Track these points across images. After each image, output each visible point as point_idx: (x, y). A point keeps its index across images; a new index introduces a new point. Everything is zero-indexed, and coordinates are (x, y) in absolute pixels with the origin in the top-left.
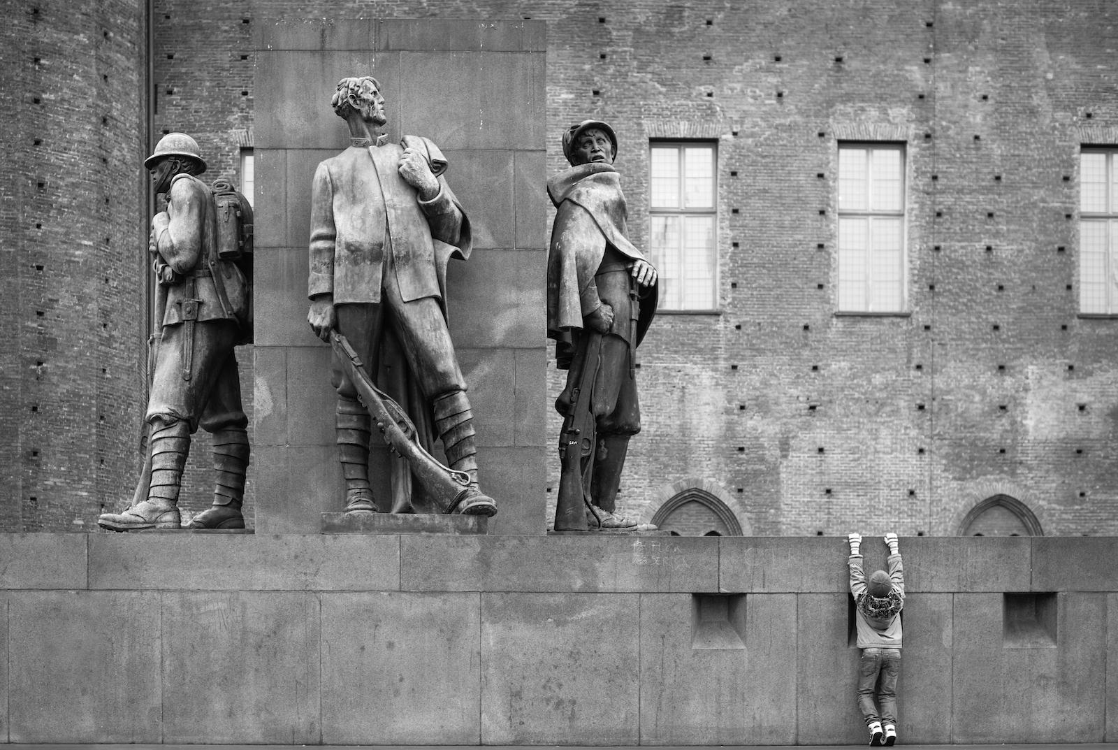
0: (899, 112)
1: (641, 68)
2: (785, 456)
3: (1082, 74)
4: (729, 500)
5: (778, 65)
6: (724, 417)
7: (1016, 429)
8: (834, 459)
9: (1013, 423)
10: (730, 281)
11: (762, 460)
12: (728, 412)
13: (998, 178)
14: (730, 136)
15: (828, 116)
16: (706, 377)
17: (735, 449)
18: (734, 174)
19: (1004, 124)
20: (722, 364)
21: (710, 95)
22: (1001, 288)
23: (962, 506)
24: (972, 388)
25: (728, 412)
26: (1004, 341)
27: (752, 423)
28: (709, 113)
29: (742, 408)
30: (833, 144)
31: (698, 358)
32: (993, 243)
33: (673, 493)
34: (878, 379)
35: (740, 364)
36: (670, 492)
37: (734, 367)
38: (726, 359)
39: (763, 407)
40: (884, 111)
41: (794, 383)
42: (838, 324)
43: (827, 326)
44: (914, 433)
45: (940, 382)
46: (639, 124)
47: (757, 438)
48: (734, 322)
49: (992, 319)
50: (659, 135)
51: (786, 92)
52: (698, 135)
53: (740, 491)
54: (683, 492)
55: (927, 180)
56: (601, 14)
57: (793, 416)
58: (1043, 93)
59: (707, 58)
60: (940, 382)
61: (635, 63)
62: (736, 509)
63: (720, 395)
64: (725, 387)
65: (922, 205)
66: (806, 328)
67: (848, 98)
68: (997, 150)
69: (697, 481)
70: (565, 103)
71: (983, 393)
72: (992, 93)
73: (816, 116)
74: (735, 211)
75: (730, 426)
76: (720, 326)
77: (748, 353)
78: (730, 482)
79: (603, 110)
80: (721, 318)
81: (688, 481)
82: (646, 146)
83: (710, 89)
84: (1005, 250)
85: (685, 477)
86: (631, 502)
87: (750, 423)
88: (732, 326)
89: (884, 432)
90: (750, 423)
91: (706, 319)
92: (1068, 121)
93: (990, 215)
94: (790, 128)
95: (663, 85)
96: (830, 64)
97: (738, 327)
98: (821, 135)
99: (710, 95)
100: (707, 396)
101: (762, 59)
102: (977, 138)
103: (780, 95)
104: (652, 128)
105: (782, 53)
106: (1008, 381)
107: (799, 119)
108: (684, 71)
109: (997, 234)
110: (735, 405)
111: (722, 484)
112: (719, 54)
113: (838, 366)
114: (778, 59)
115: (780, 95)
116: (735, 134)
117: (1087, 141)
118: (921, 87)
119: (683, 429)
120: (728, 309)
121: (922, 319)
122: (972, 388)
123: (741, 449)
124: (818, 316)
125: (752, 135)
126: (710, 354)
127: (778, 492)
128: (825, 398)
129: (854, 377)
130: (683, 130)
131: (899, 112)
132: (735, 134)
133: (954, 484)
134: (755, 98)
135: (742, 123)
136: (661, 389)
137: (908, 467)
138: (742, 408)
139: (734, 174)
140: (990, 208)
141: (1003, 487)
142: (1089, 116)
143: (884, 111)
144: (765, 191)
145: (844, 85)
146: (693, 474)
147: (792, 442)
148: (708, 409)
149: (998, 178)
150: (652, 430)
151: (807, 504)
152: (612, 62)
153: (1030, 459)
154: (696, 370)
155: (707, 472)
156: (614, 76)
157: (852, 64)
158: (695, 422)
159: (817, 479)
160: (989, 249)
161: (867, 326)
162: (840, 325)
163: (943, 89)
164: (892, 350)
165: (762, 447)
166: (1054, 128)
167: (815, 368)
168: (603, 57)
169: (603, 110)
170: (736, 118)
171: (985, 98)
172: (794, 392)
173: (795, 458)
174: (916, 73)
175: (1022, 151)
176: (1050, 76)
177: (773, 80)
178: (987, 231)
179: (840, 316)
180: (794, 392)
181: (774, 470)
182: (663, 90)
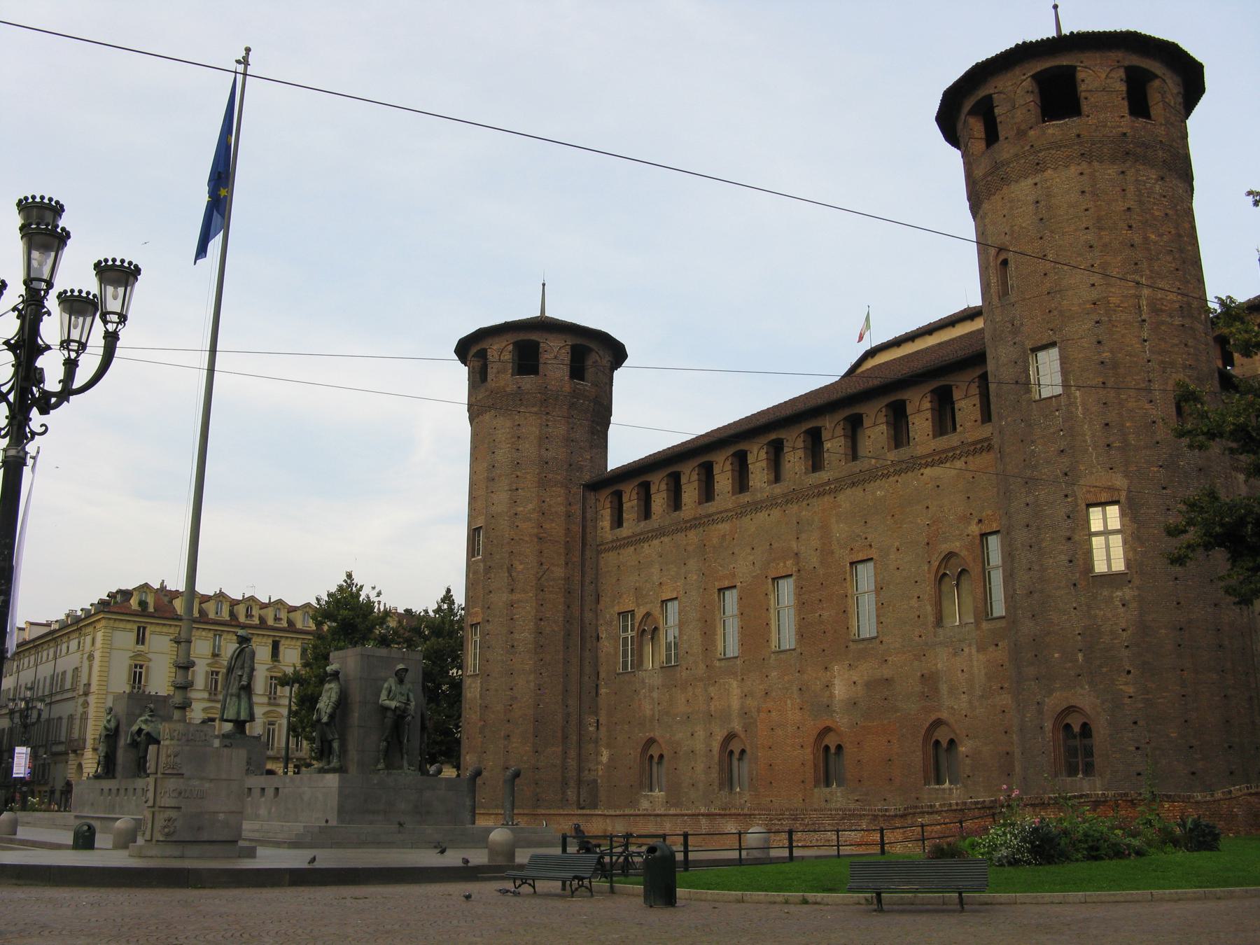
0: (789, 563)
7: (832, 696)
17: (745, 713)
23: (815, 733)
27: (749, 701)
28: (734, 575)
45: (805, 677)
84: (826, 614)
104: (718, 585)
113: (774, 674)
119: (729, 706)
141: (828, 723)
157: (774, 546)
173: (763, 715)
174: (794, 545)
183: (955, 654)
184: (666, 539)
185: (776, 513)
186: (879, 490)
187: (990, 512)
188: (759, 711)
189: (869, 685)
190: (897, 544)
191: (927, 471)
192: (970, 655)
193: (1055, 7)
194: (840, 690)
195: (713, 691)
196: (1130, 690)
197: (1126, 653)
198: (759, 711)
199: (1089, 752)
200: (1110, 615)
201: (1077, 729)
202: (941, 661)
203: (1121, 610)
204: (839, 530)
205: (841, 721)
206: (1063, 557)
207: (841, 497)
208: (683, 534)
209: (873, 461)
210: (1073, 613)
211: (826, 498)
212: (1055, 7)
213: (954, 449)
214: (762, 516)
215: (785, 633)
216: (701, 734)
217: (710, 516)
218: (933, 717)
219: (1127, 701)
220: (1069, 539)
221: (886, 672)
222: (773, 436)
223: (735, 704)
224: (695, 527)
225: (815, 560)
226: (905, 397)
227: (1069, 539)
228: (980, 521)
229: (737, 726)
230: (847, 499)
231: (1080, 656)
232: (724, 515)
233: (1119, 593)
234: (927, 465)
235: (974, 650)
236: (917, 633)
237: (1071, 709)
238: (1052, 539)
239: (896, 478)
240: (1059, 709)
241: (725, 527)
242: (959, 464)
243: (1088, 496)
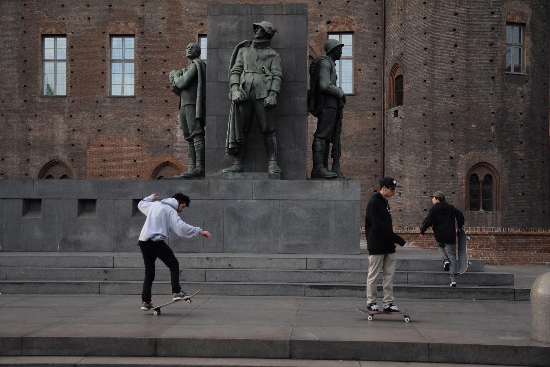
0: (132, 25)
1: (39, 9)
2: (89, 148)
3: (199, 9)
4: (68, 164)
5: (88, 8)
6: (67, 134)
8: (107, 148)
9: (172, 135)
10: (70, 85)
11: (80, 149)
12: (68, 132)
13: (168, 47)
14: (70, 34)
15: (106, 26)
16: (61, 119)
17: (71, 145)
18: (72, 47)
19: (170, 28)
20: (67, 115)
21: (64, 19)
22: (168, 87)
23: (154, 166)
24: (157, 123)
25: (68, 132)
26: (169, 106)
27: (77, 135)
28: (63, 25)
29: (74, 130)
30: (108, 36)
31: (58, 112)
32: (165, 70)
33: (48, 161)
34: (123, 120)
35: (73, 115)
36: (47, 160)
37: (71, 116)
38: (68, 113)
40: (126, 24)
41: (93, 122)
42: (109, 100)
43: (105, 101)
44: (136, 139)
45: (145, 121)
46: (38, 29)
47: (79, 141)
48: (71, 100)
49: (165, 98)
50: (45, 33)
51: (91, 17)
52: (59, 33)
53: (73, 160)
54: (52, 161)
55: (142, 48)
57: (92, 133)
58: (185, 16)
59: (63, 6)
60: (145, 121)
61: (37, 7)
62: (71, 167)
63: (66, 125)
64: (68, 123)
65: (140, 57)
66: (97, 102)
67: (113, 19)
68: (168, 37)
69: (57, 156)
70: (11, 22)
71: (161, 124)
72: (166, 17)
73: (102, 26)
74: (72, 60)
75: (69, 137)
76: (66, 101)
77: (76, 111)
78: (69, 157)
79: (25, 25)
80: (67, 98)
81: (54, 156)
82: (40, 37)
83: (64, 16)
85: (52, 155)
86: (33, 164)
87: (76, 136)
88: (70, 101)
89: (125, 139)
90: (76, 136)
91: (61, 99)
92: (194, 26)
93: (165, 61)
94: (92, 30)
95: (47, 15)
96: (107, 7)
97: (73, 102)
98: (104, 33)
99: (64, 19)
100: (61, 126)
101: (83, 6)
102: (160, 33)
103: (89, 19)
104: (42, 31)
105: (90, 3)
106: (171, 120)
107: (95, 27)
108: (54, 10)
109: (167, 68)
110: (71, 129)
111: (66, 158)
113: (109, 115)
114: (88, 6)
115: (89, 19)
116: (72, 33)
117: (201, 33)
119: (53, 138)
120: (69, 95)
121: (139, 98)
122: (157, 123)
123: (73, 145)
124: (102, 97)
125: (79, 33)
126: (62, 112)
127: (86, 161)
128: (104, 127)
129: (114, 119)
130: (54, 31)
132: (72, 33)
133: (150, 158)
134: (80, 20)
135: (75, 29)
136: (44, 124)
137: (134, 151)
138: (74, 130)
139: (72, 47)
140: (165, 58)
141: (168, 159)
142: (202, 24)
143: (126, 24)
144: (83, 53)
145: (112, 15)
146: (56, 154)
147: (91, 143)
148: (61, 131)
149: (168, 47)
150: (41, 138)
151: (96, 165)
152: (28, 7)
153: (178, 148)
154: (57, 117)
155: (60, 153)
156: (29, 12)
157: (115, 7)
158: (56, 135)
159: (100, 156)
160: (164, 73)
162: (109, 101)
163: (148, 15)
164: (128, 110)
165: (80, 144)
166: (189, 29)
167: (100, 116)
168: (25, 5)
169: (25, 25)
170: (73, 27)
171: (163, 18)
172: (93, 125)
173: (94, 148)
174: (138, 11)
175: (177, 37)
176: (187, 10)
177: (86, 13)
178: (164, 67)
180: (93, 125)
181: (85, 153)
182: (47, 17)
187: (338, 17)
188: (89, 144)
195: (31, 123)
196: (522, 154)
197: (521, 130)
198: (89, 144)
199: (487, 195)
200: (514, 102)
201: (481, 178)
203: (521, 100)
206: (485, 57)
210: (490, 97)
215: (123, 82)
219: (520, 162)
220: (492, 44)
223: (61, 135)
225: (161, 27)
227: (492, 44)
228: (329, 22)
229: (62, 155)
231: (493, 128)
233: (520, 88)
237: (482, 164)
238: (479, 42)
240: (473, 164)
243: (509, 16)
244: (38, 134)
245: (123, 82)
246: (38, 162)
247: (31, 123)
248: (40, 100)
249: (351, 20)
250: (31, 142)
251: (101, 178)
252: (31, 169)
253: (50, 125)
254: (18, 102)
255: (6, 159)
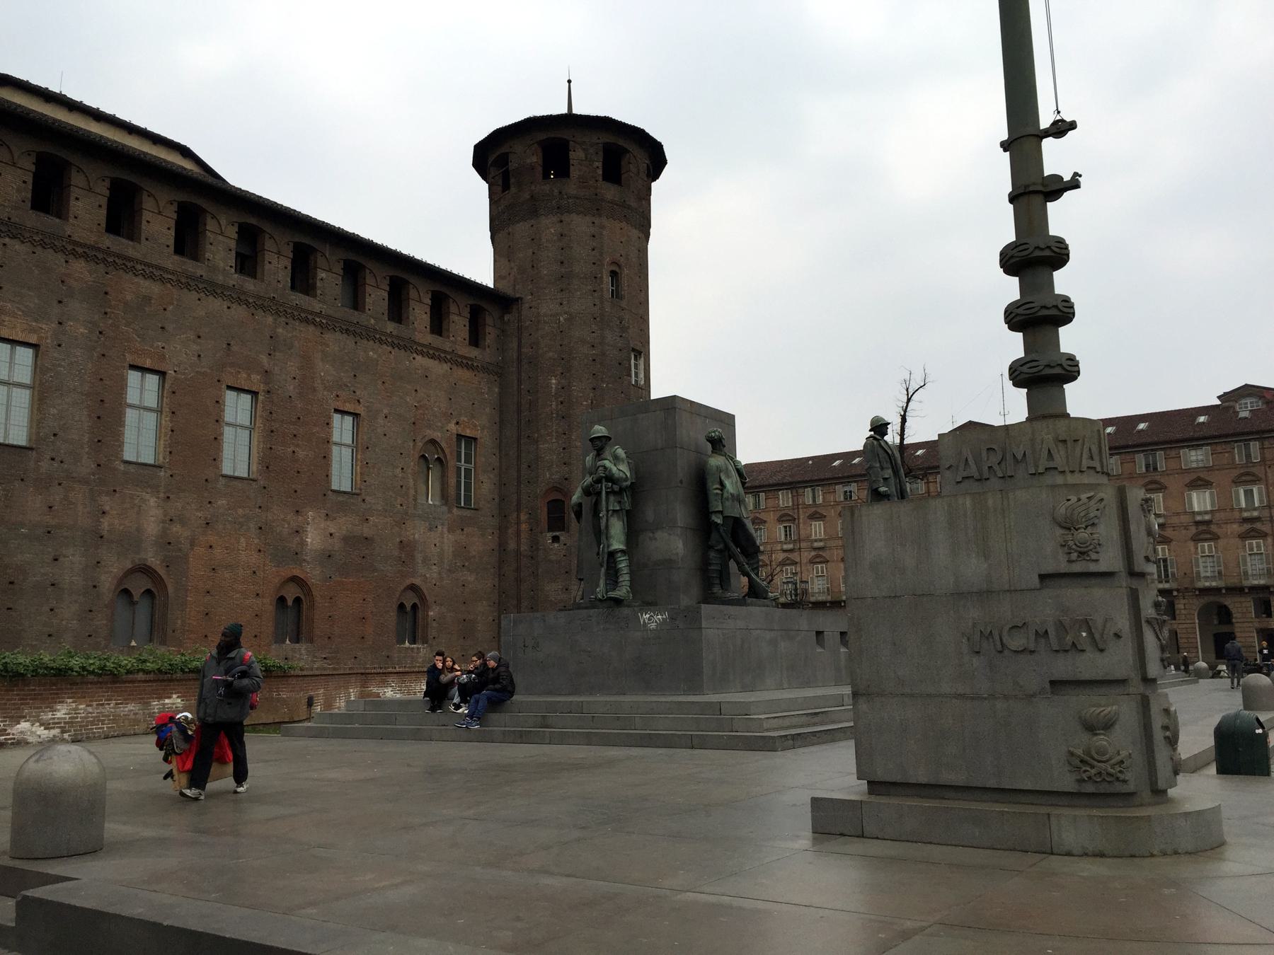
4: (162, 572)
7: (303, 543)
12: (163, 522)
16: (153, 502)
17: (166, 543)
20: (162, 495)
25: (163, 522)
27: (176, 528)
30: (224, 386)
32: (297, 449)
34: (240, 511)
39: (183, 521)
40: (249, 375)
44: (256, 541)
48: (170, 473)
56: (109, 289)
63: (159, 512)
84: (301, 454)
89: (242, 540)
104: (130, 358)
109: (298, 446)
112: (170, 327)
113: (222, 502)
118: (267, 367)
119: (138, 530)
131: (256, 377)
141: (297, 572)
143: (249, 375)
154: (148, 496)
155: (150, 554)
157: (234, 348)
161: (236, 483)
174: (264, 359)
177: (195, 347)
179: (223, 476)
183: (430, 529)
184: (16, 246)
185: (239, 312)
186: (371, 351)
188: (193, 544)
189: (346, 539)
190: (385, 411)
191: (419, 358)
192: (442, 533)
193: (569, 82)
194: (313, 539)
195: (106, 502)
198: (192, 544)
202: (417, 531)
204: (324, 370)
205: (313, 573)
207: (329, 336)
208: (61, 258)
209: (372, 321)
211: (311, 328)
212: (569, 82)
213: (445, 352)
214: (216, 304)
215: (237, 454)
216: (74, 558)
217: (130, 259)
218: (408, 582)
221: (367, 531)
222: (253, 221)
223: (151, 527)
224: (96, 260)
225: (291, 388)
226: (411, 280)
230: (336, 342)
232: (157, 273)
234: (422, 354)
235: (445, 530)
236: (399, 501)
239: (389, 348)
241: (154, 288)
242: (446, 367)
244: (116, 522)
245: (237, 454)
246: (114, 567)
247: (106, 502)
248: (122, 467)
249: (475, 426)
250: (105, 533)
251: (208, 598)
252: (103, 578)
253: (136, 509)
254: (86, 466)
255: (61, 559)
